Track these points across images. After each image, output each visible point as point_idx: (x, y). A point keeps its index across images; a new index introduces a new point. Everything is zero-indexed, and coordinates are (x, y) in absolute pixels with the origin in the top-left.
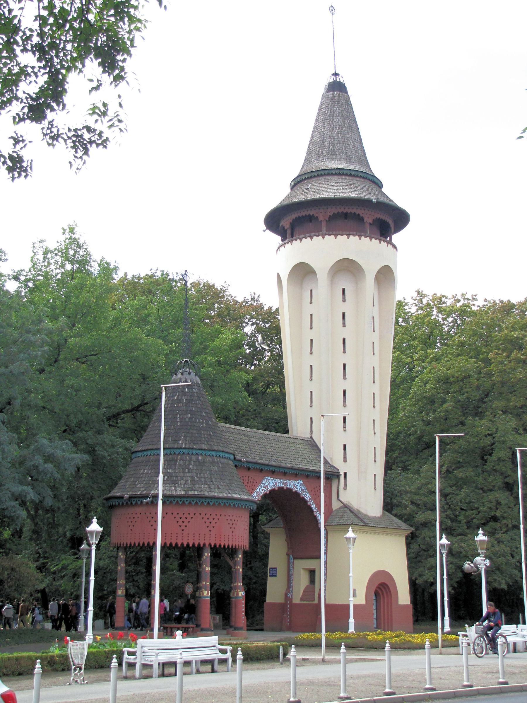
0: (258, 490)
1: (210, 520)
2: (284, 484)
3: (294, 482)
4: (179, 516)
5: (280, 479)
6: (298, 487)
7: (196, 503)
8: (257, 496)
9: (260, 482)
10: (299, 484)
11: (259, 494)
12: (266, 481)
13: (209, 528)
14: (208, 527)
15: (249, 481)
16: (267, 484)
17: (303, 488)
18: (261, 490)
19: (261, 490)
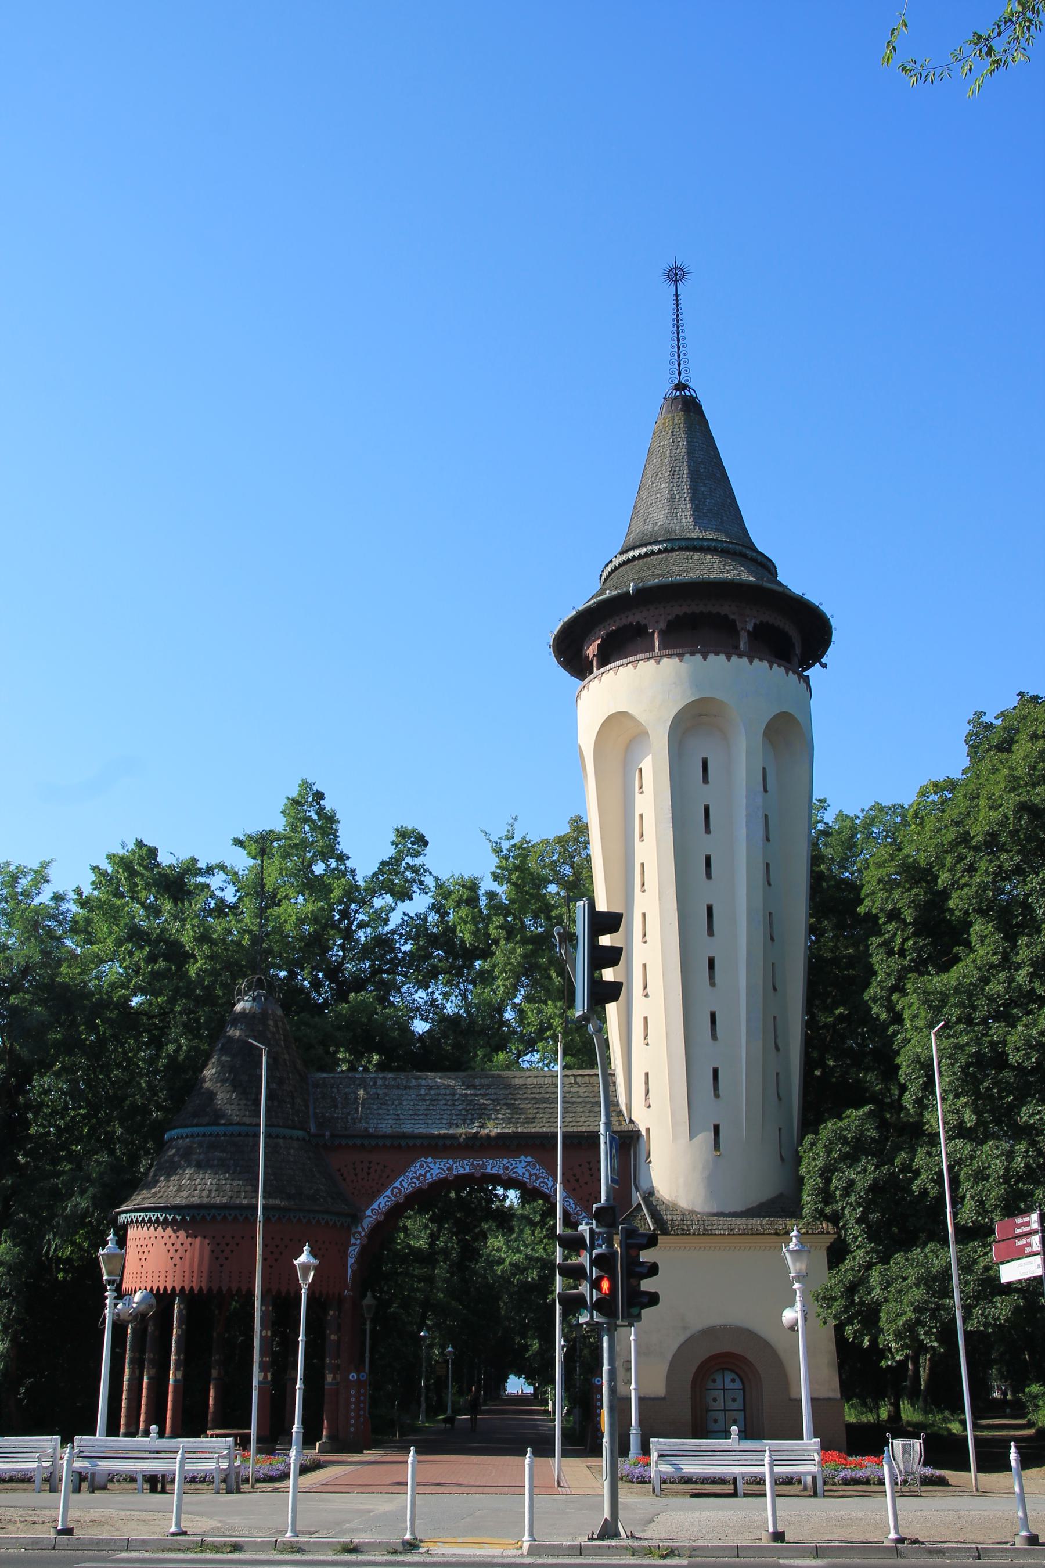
0: (397, 1184)
2: (475, 1167)
3: (505, 1161)
4: (150, 1245)
5: (463, 1159)
6: (520, 1171)
7: (225, 1217)
8: (395, 1196)
9: (403, 1171)
10: (523, 1164)
12: (422, 1166)
13: (174, 1261)
16: (423, 1172)
17: (533, 1171)
19: (405, 1185)
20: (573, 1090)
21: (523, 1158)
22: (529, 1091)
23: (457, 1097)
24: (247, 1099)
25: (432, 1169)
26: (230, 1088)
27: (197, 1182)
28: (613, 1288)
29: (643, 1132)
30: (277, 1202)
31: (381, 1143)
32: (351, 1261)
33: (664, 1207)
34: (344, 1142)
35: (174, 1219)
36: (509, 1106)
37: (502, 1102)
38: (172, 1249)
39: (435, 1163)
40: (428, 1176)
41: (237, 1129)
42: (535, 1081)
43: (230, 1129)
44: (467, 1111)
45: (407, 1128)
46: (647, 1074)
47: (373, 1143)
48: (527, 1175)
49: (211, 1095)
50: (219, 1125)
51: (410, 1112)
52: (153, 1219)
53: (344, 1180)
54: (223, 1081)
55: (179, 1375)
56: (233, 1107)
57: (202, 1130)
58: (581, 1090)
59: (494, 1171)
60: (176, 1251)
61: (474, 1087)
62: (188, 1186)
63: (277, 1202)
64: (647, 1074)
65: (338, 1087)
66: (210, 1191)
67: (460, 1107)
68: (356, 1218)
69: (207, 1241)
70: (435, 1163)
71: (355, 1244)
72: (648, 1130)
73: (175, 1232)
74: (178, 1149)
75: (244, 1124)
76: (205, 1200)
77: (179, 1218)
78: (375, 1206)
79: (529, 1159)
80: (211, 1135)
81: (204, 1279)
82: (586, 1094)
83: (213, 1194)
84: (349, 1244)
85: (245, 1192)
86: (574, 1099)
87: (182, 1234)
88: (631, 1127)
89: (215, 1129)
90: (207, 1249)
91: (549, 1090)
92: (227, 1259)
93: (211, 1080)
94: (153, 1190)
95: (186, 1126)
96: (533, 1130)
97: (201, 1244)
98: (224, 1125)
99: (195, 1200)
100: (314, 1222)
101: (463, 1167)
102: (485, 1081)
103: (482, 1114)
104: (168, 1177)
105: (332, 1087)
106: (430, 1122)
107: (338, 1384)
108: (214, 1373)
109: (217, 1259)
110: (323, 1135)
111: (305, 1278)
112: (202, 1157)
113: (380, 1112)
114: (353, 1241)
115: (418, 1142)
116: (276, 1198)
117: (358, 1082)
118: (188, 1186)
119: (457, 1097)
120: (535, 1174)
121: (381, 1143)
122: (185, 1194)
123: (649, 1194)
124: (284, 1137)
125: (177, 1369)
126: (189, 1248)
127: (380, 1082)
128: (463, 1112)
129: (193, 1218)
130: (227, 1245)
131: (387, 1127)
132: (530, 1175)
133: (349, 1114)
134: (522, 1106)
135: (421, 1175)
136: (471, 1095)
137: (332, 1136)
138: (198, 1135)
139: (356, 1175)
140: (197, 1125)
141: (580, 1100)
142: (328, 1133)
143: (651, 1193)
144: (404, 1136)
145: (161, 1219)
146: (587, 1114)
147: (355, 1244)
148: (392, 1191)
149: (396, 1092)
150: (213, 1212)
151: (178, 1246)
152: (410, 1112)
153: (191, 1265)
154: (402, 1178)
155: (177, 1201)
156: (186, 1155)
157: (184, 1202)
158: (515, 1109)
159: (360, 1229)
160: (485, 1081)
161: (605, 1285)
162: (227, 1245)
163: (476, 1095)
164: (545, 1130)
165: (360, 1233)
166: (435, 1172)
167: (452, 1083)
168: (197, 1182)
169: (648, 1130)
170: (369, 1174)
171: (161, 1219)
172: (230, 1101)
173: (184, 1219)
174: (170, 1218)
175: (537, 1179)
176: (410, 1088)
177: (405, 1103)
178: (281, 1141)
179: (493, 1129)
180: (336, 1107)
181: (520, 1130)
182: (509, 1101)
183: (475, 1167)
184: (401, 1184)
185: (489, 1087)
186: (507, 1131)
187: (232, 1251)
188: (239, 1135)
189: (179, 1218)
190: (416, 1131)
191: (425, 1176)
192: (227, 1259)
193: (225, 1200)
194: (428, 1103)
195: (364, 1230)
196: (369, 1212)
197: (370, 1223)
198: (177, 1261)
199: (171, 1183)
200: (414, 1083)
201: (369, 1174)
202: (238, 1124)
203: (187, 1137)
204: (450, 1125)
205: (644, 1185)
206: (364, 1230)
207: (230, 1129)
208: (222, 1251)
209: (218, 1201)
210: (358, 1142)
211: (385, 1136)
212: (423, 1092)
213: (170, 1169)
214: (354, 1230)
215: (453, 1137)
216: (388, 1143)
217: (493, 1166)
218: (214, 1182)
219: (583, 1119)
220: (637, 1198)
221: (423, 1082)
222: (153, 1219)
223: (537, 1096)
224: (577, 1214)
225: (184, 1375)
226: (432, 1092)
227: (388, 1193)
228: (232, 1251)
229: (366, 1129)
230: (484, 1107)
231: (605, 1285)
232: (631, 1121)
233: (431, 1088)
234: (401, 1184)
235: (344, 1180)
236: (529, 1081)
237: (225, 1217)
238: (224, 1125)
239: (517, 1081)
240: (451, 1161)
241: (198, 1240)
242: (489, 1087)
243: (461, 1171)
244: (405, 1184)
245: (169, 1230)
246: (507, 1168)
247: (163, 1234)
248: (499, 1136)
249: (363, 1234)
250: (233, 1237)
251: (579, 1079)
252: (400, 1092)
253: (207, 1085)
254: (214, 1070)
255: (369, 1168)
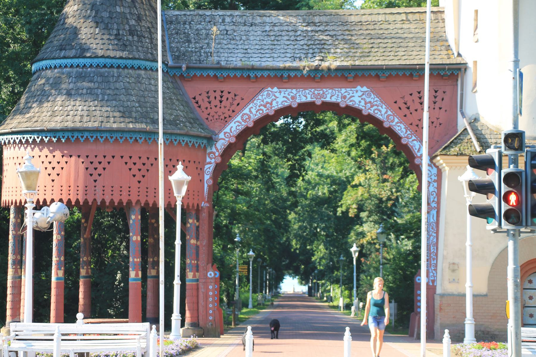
0: (246, 111)
1: (94, 165)
2: (316, 96)
3: (343, 90)
5: (305, 89)
6: (357, 99)
8: (245, 121)
9: (252, 100)
10: (360, 94)
11: (249, 117)
12: (268, 95)
13: (51, 177)
14: (49, 175)
15: (224, 99)
16: (269, 100)
17: (368, 100)
18: (254, 111)
19: (254, 111)
20: (405, 26)
21: (359, 88)
22: (365, 28)
23: (299, 33)
24: (110, 34)
25: (277, 97)
26: (92, 24)
27: (69, 108)
28: (518, 201)
29: (470, 65)
30: (143, 126)
31: (232, 74)
32: (207, 177)
33: (488, 132)
34: (198, 74)
35: (50, 141)
36: (346, 41)
37: (340, 38)
38: (50, 167)
39: (280, 92)
40: (274, 103)
41: (102, 61)
42: (369, 18)
43: (95, 61)
44: (308, 46)
45: (255, 62)
46: (476, 11)
47: (225, 74)
48: (363, 103)
49: (75, 31)
50: (85, 57)
51: (257, 47)
52: (30, 140)
53: (199, 107)
54: (86, 18)
55: (61, 273)
56: (97, 41)
57: (69, 61)
58: (412, 26)
59: (334, 100)
60: (53, 168)
61: (314, 24)
62: (60, 112)
63: (143, 126)
64: (476, 11)
65: (190, 23)
66: (82, 116)
67: (302, 43)
68: (211, 140)
69: (81, 160)
70: (280, 92)
71: (210, 163)
72: (475, 63)
73: (51, 152)
74: (48, 79)
75: (108, 57)
76: (78, 125)
77: (55, 140)
78: (227, 130)
79: (365, 89)
80: (78, 66)
81: (81, 192)
82: (417, 31)
83: (85, 119)
84: (204, 163)
85: (114, 117)
86: (405, 35)
87: (58, 153)
88: (459, 60)
89: (81, 61)
90: (82, 167)
91: (383, 26)
92: (100, 175)
93: (74, 16)
94: (27, 116)
95: (54, 58)
96: (369, 63)
97: (76, 162)
98: (90, 57)
99: (70, 125)
100: (176, 143)
101: (305, 95)
102: (324, 19)
103: (322, 48)
104: (41, 103)
105: (185, 23)
106: (276, 55)
107: (197, 280)
108: (83, 272)
109: (91, 175)
110: (180, 68)
111: (179, 192)
112: (71, 86)
113: (230, 46)
114: (208, 160)
115: (266, 74)
116: (142, 123)
117: (208, 19)
118: (60, 112)
119: (299, 33)
120: (370, 102)
121: (232, 74)
122: (59, 119)
123: (474, 121)
124: (145, 69)
125: (58, 268)
126: (64, 165)
127: (228, 20)
128: (305, 47)
129: (68, 139)
130: (100, 163)
131: (236, 60)
132: (366, 103)
133: (202, 48)
134: (357, 42)
135: (267, 103)
136: (312, 31)
137: (188, 68)
138: (66, 67)
139: (210, 103)
140: (64, 58)
141: (411, 36)
142: (184, 66)
143: (476, 120)
144: (253, 69)
145: (38, 140)
146: (419, 49)
147: (210, 163)
148: (242, 117)
149: (243, 28)
150: (86, 134)
151: (54, 164)
152: (257, 47)
153: (68, 180)
154: (251, 105)
155: (52, 125)
156: (56, 84)
157: (59, 126)
158: (354, 45)
159: (214, 150)
160: (324, 19)
161: (513, 198)
162: (100, 163)
163: (317, 32)
164: (380, 63)
165: (214, 153)
166: (280, 99)
167: (293, 20)
168: (69, 108)
169: (475, 63)
170: (221, 102)
171: (38, 140)
172: (94, 36)
173: (59, 140)
174: (46, 140)
175: (372, 106)
176: (255, 25)
177: (252, 38)
178: (142, 72)
179: (332, 62)
180: (189, 41)
181: (357, 63)
182: (346, 37)
183: (316, 96)
184: (250, 111)
185: (327, 23)
186: (345, 64)
187: (104, 169)
188: (105, 66)
189: (55, 140)
190: (264, 64)
191: (271, 104)
192: (100, 175)
193: (96, 124)
194: (273, 38)
195: (217, 150)
196: (221, 136)
197: (223, 144)
198: (54, 176)
199: (44, 109)
200: (258, 20)
201: (221, 102)
202: (102, 57)
203: (55, 67)
204: (294, 58)
205: (469, 111)
206: (217, 150)
207: (95, 61)
208: (96, 169)
209: (90, 125)
210: (212, 73)
211: (235, 69)
212: (267, 28)
213: (42, 97)
214: (209, 150)
215: (297, 69)
216: (238, 74)
217: (333, 95)
218: (85, 108)
219: (414, 53)
220: (462, 123)
221: (267, 20)
222: (30, 140)
223: (372, 32)
224: (407, 137)
225: (65, 272)
226: (276, 29)
227: (239, 118)
228: (104, 169)
229: (218, 63)
230: (323, 43)
231: (513, 198)
232: (459, 55)
233: (275, 25)
234: (250, 111)
235: (199, 107)
236: (364, 18)
237: (116, 139)
238: (90, 57)
239: (353, 19)
240: (294, 91)
241: (73, 158)
242: (327, 23)
243: (304, 100)
244: (253, 111)
245: (46, 151)
246: (345, 97)
247: (40, 154)
248: (339, 69)
249: (217, 154)
250: (105, 157)
251: (410, 16)
252: (247, 28)
253: (70, 21)
254: (76, 8)
255: (221, 97)
